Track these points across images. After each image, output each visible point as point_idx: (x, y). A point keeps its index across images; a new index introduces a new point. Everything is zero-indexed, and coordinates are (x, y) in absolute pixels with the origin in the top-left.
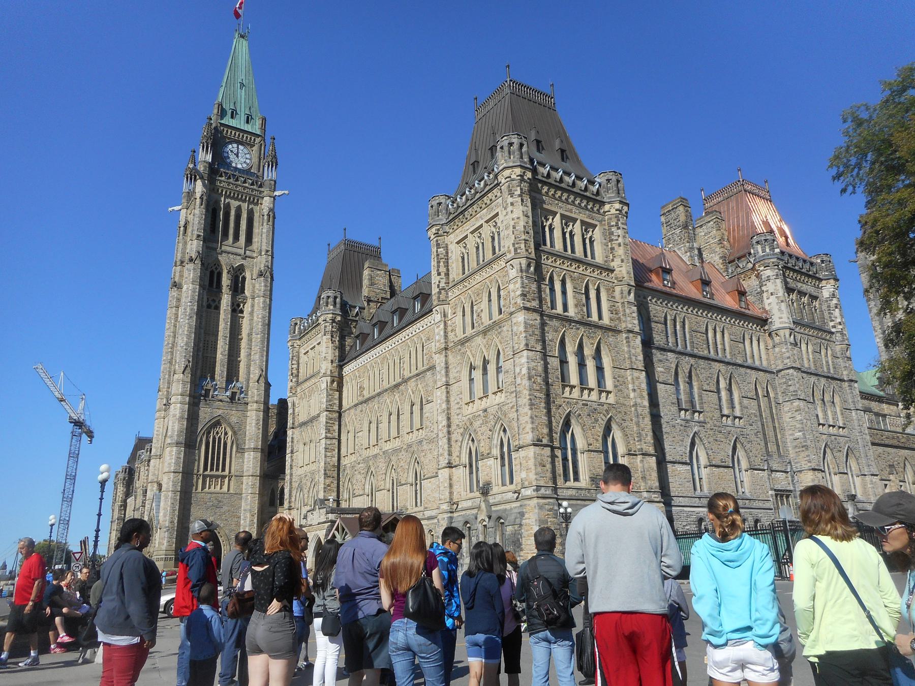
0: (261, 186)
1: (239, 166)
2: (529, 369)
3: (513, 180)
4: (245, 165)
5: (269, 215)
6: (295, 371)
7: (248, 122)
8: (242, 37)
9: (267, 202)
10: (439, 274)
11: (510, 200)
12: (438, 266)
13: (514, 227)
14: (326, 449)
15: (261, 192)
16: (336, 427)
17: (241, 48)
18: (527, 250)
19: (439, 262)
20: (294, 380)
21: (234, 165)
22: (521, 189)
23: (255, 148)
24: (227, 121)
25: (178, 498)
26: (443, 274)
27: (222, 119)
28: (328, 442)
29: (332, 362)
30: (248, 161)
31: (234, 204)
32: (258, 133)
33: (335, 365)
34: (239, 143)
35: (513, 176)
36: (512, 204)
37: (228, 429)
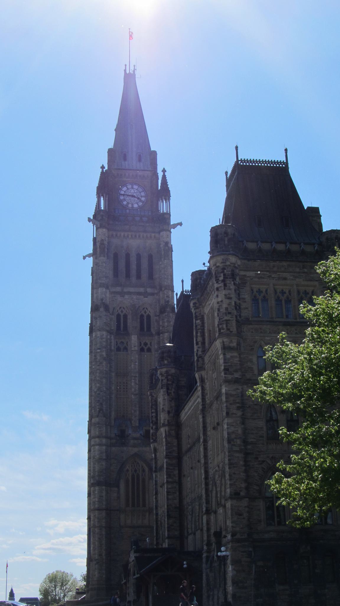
2: (228, 434)
3: (218, 267)
6: (154, 419)
7: (140, 160)
10: (197, 344)
11: (216, 285)
12: (197, 337)
13: (219, 310)
14: (167, 492)
16: (176, 472)
18: (228, 329)
19: (197, 333)
20: (154, 427)
22: (224, 275)
25: (104, 533)
26: (200, 343)
28: (169, 487)
29: (169, 412)
33: (171, 415)
35: (218, 264)
36: (218, 289)
37: (145, 466)
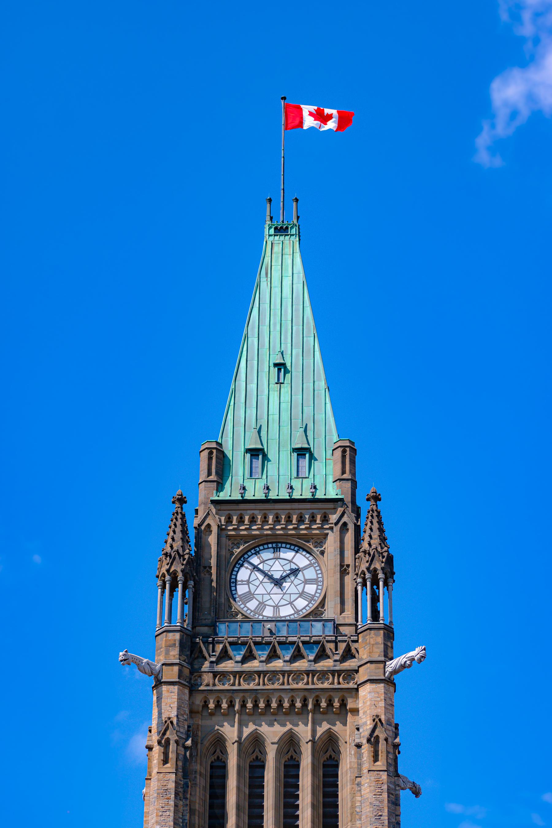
0: (348, 654)
1: (286, 612)
4: (301, 603)
5: (373, 740)
8: (281, 231)
9: (369, 701)
15: (350, 674)
17: (283, 269)
21: (268, 613)
23: (332, 542)
24: (243, 483)
27: (220, 486)
30: (311, 589)
31: (272, 732)
32: (332, 492)
34: (276, 543)
